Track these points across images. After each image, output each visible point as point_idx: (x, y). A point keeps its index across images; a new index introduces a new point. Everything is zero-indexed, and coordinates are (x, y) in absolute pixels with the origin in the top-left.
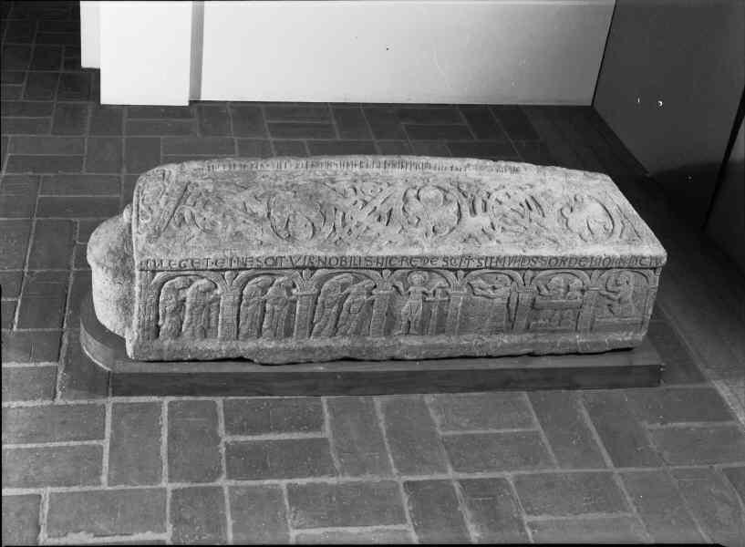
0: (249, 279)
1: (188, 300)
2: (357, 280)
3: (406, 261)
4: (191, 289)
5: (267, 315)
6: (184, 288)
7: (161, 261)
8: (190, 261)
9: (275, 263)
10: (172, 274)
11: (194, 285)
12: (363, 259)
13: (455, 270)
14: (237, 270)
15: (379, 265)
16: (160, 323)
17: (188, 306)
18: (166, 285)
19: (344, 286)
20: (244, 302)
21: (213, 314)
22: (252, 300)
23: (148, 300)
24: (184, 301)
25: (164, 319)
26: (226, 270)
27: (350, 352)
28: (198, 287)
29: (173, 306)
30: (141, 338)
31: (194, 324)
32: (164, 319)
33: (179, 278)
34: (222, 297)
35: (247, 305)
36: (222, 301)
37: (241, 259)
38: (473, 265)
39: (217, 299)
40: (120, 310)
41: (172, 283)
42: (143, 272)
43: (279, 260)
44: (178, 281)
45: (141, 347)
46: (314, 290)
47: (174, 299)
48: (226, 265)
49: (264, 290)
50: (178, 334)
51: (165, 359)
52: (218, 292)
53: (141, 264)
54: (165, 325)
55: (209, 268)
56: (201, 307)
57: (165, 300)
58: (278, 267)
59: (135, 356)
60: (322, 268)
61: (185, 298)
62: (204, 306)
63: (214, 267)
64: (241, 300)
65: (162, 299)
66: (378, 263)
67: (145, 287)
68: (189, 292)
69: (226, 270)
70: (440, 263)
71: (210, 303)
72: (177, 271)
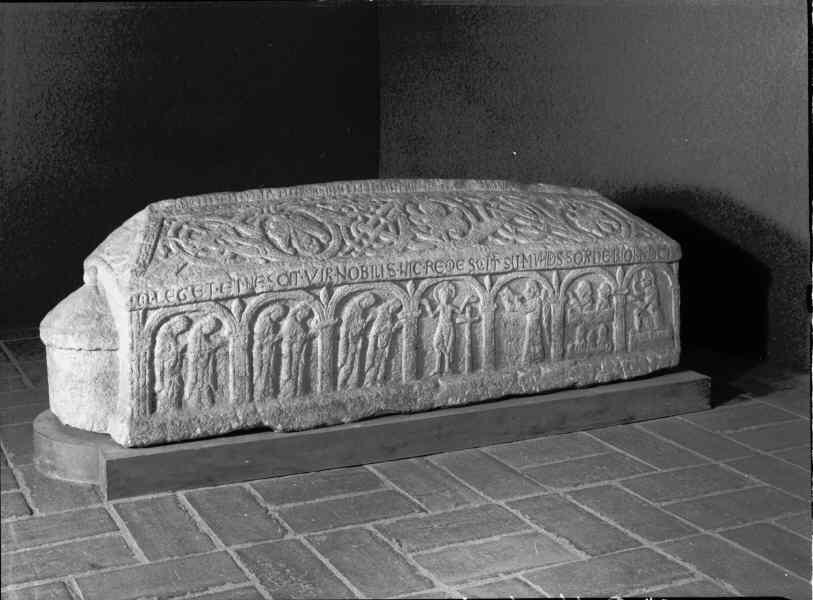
0: (259, 309)
1: (190, 348)
2: (378, 301)
3: (431, 266)
4: (192, 332)
5: (285, 362)
6: (182, 332)
7: (156, 296)
8: (190, 289)
9: (290, 282)
10: (168, 312)
11: (196, 326)
12: (385, 266)
13: (477, 277)
14: (242, 299)
15: (403, 276)
16: (157, 387)
17: (190, 356)
18: (163, 329)
19: (365, 312)
20: (257, 344)
21: (220, 367)
22: (266, 340)
23: (142, 354)
24: (185, 350)
25: (162, 380)
26: (232, 298)
27: (387, 402)
28: (201, 327)
29: (173, 359)
30: (135, 415)
31: (199, 384)
32: (162, 380)
33: (177, 318)
34: (231, 340)
35: (261, 347)
36: (230, 345)
37: (250, 280)
38: (500, 268)
39: (224, 344)
40: (100, 390)
41: (170, 327)
42: (135, 313)
43: (293, 275)
44: (177, 323)
45: (138, 424)
46: (331, 321)
47: (173, 348)
48: (233, 292)
49: (276, 326)
50: (179, 402)
51: (169, 439)
52: (225, 332)
53: (131, 300)
54: (164, 391)
55: (213, 297)
56: (206, 356)
57: (163, 351)
58: (293, 286)
59: (132, 439)
60: (342, 284)
61: (186, 346)
62: (209, 354)
63: (219, 295)
64: (251, 341)
65: (157, 350)
66: (401, 272)
67: (137, 335)
68: (190, 338)
69: (232, 298)
70: (466, 267)
71: (216, 349)
72: (175, 305)
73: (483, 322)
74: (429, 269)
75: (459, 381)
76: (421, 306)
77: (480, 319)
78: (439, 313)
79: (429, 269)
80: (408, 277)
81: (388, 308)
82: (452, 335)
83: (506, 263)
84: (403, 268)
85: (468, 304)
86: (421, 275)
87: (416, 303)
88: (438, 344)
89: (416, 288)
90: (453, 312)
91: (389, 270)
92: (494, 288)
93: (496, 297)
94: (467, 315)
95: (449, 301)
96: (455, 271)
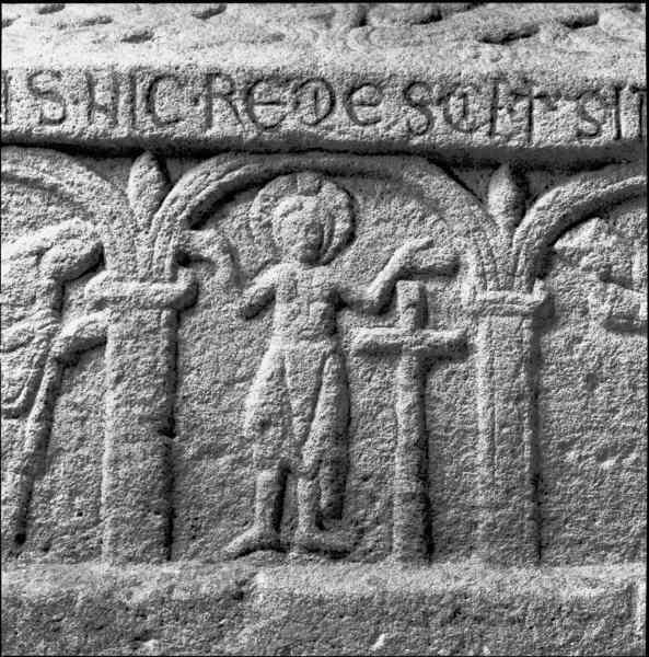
3: (227, 96)
15: (101, 122)
66: (92, 107)
70: (391, 120)
73: (480, 359)
74: (217, 104)
75: (345, 582)
76: (184, 259)
77: (461, 349)
78: (267, 301)
79: (217, 104)
80: (122, 131)
81: (40, 253)
82: (327, 393)
83: (583, 114)
84: (101, 97)
85: (407, 273)
86: (182, 131)
87: (163, 249)
88: (264, 425)
89: (168, 183)
90: (338, 302)
91: (38, 93)
92: (531, 217)
93: (544, 262)
94: (404, 319)
95: (316, 255)
96: (341, 127)
